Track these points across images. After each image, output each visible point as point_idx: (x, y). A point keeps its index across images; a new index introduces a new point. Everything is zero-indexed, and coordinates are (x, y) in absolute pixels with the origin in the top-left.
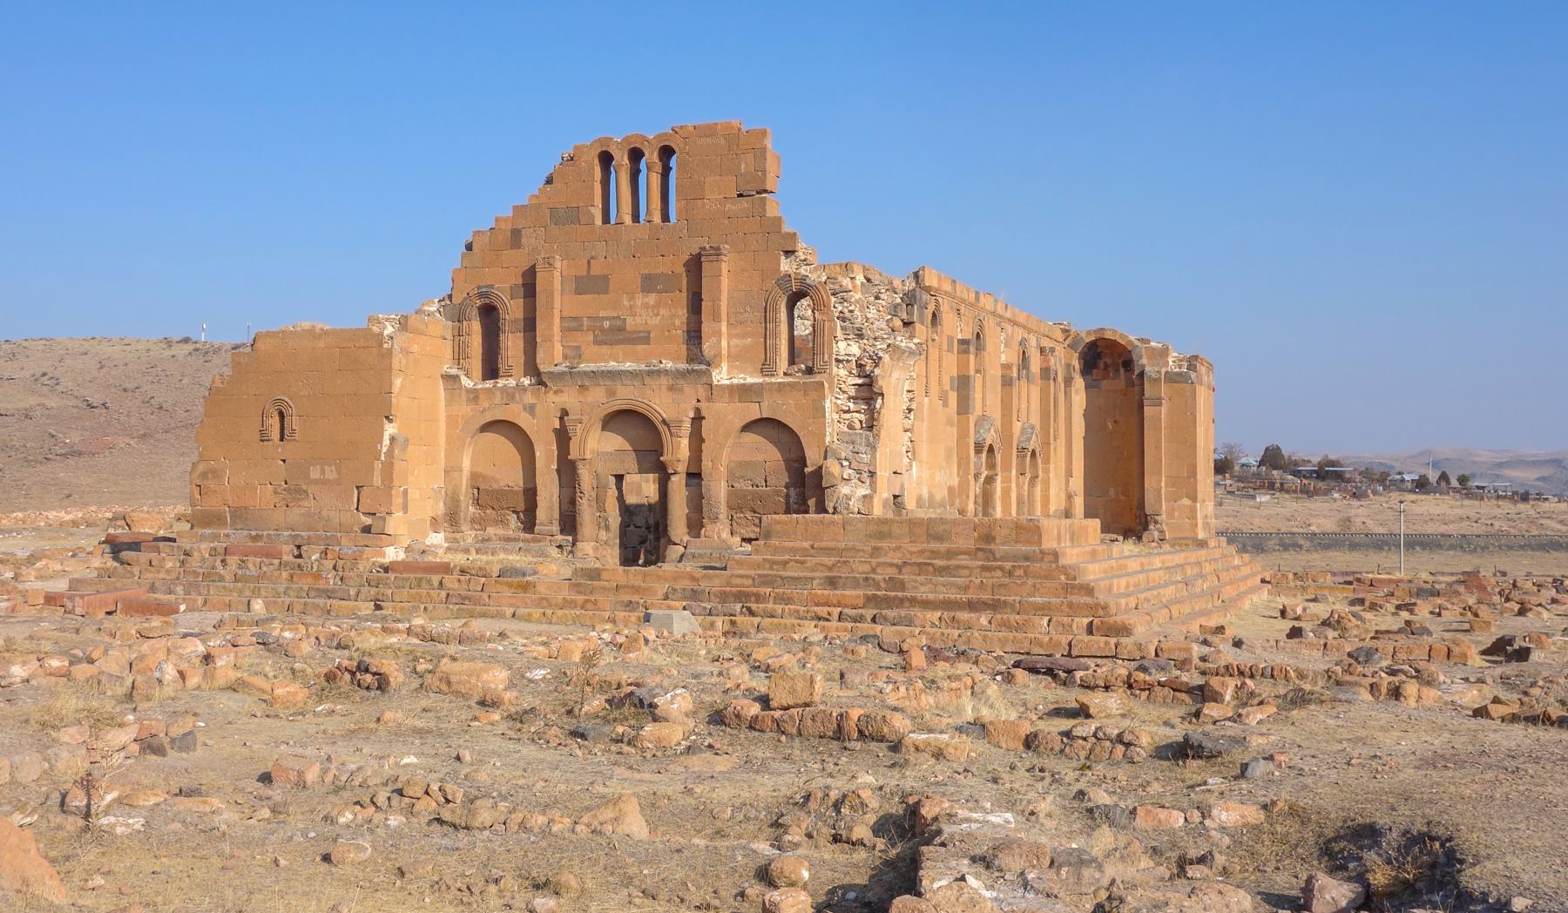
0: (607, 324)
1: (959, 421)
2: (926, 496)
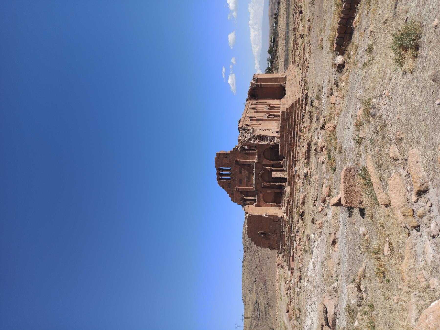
0: (247, 179)
1: (264, 121)
2: (276, 127)
